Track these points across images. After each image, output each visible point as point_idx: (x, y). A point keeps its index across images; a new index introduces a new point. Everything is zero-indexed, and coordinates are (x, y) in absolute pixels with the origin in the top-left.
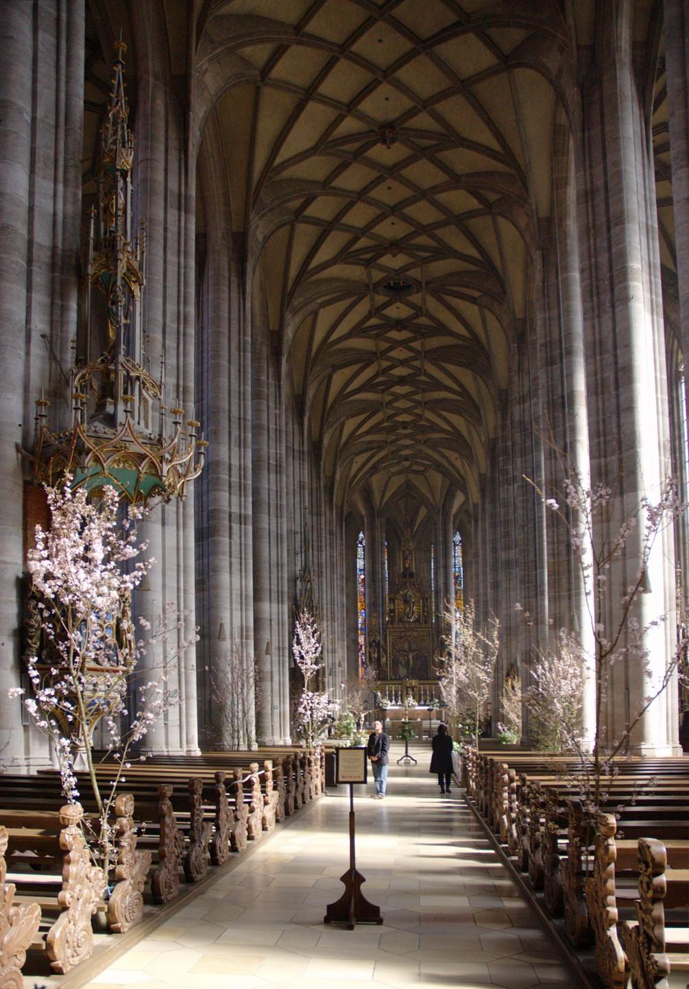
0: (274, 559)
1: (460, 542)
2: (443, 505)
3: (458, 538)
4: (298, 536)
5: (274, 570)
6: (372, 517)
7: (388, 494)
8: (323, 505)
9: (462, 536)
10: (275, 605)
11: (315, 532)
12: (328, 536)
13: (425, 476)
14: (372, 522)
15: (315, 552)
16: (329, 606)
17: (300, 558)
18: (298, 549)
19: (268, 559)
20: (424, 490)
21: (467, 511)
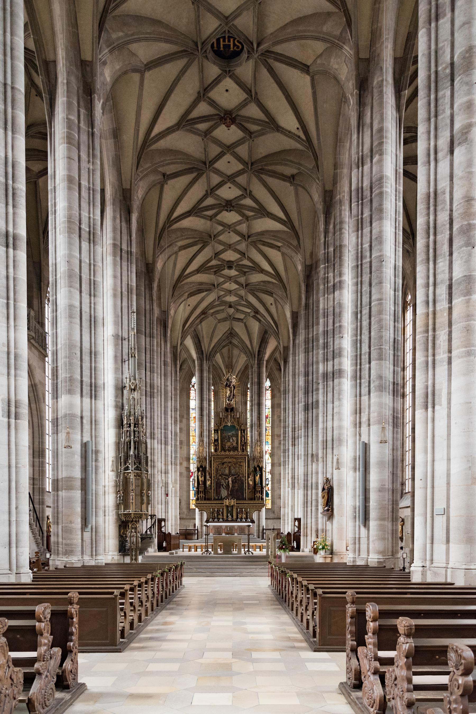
0: (86, 345)
1: (270, 387)
2: (259, 351)
3: (267, 384)
4: (125, 343)
5: (86, 358)
6: (201, 360)
7: (215, 341)
8: (155, 327)
9: (271, 383)
10: (87, 400)
11: (148, 353)
12: (163, 367)
13: (245, 324)
14: (201, 366)
15: (148, 373)
16: (163, 431)
17: (127, 366)
18: (125, 357)
19: (79, 344)
20: (245, 337)
21: (276, 360)
